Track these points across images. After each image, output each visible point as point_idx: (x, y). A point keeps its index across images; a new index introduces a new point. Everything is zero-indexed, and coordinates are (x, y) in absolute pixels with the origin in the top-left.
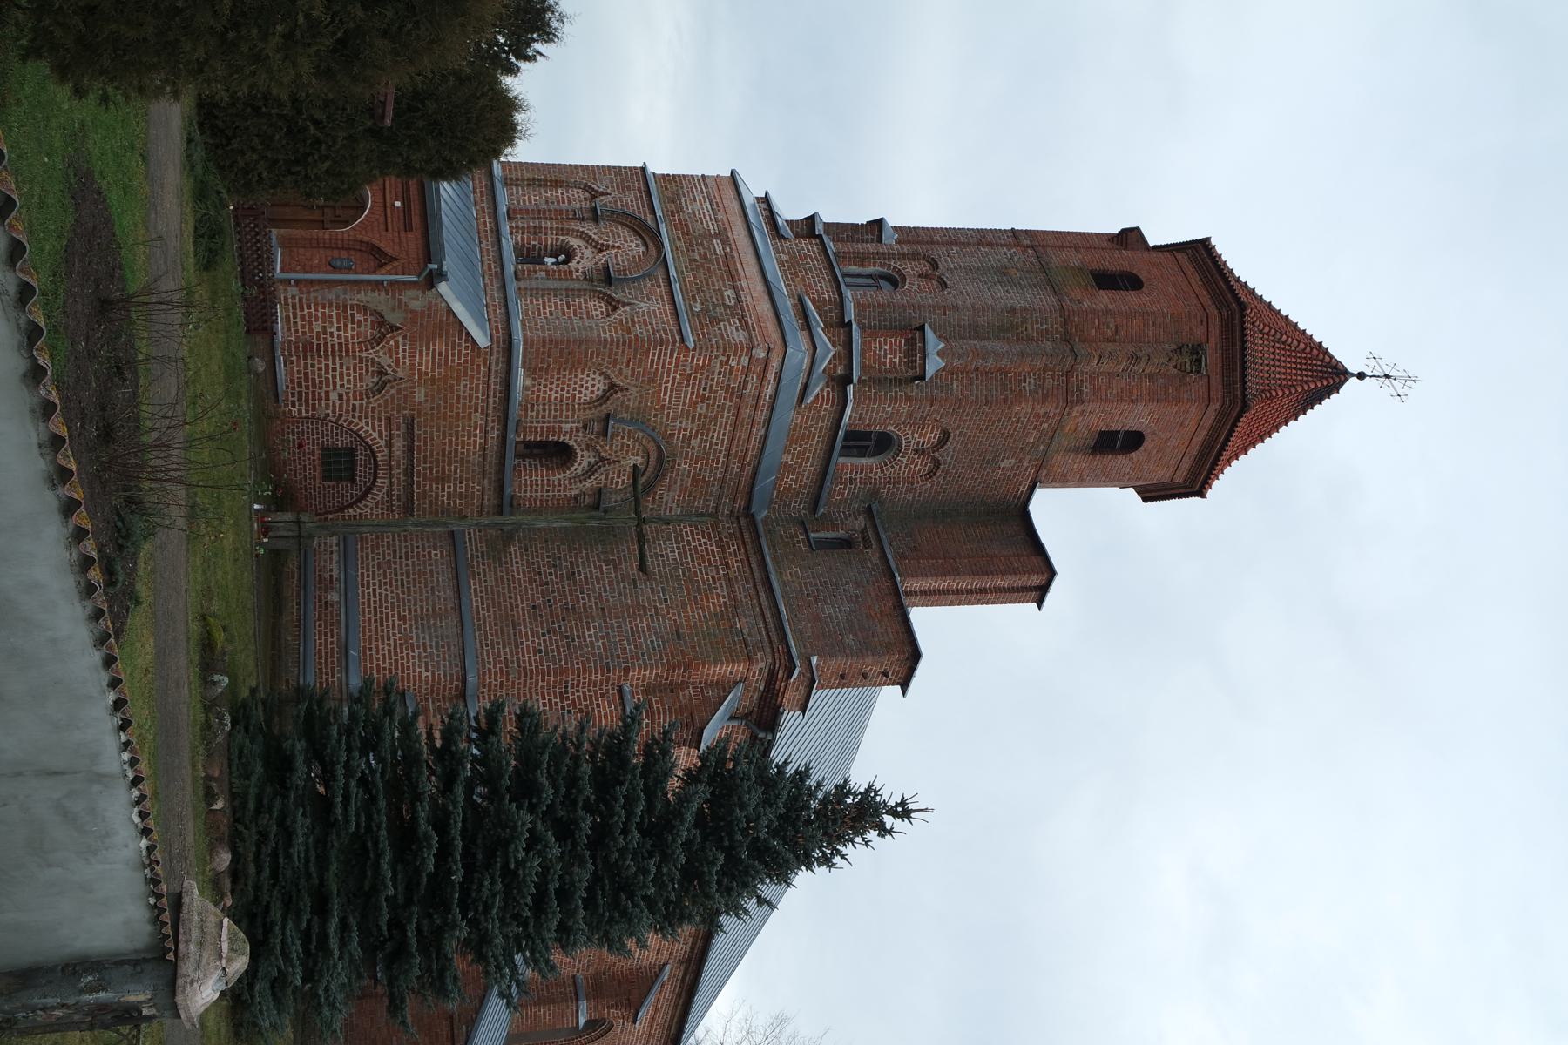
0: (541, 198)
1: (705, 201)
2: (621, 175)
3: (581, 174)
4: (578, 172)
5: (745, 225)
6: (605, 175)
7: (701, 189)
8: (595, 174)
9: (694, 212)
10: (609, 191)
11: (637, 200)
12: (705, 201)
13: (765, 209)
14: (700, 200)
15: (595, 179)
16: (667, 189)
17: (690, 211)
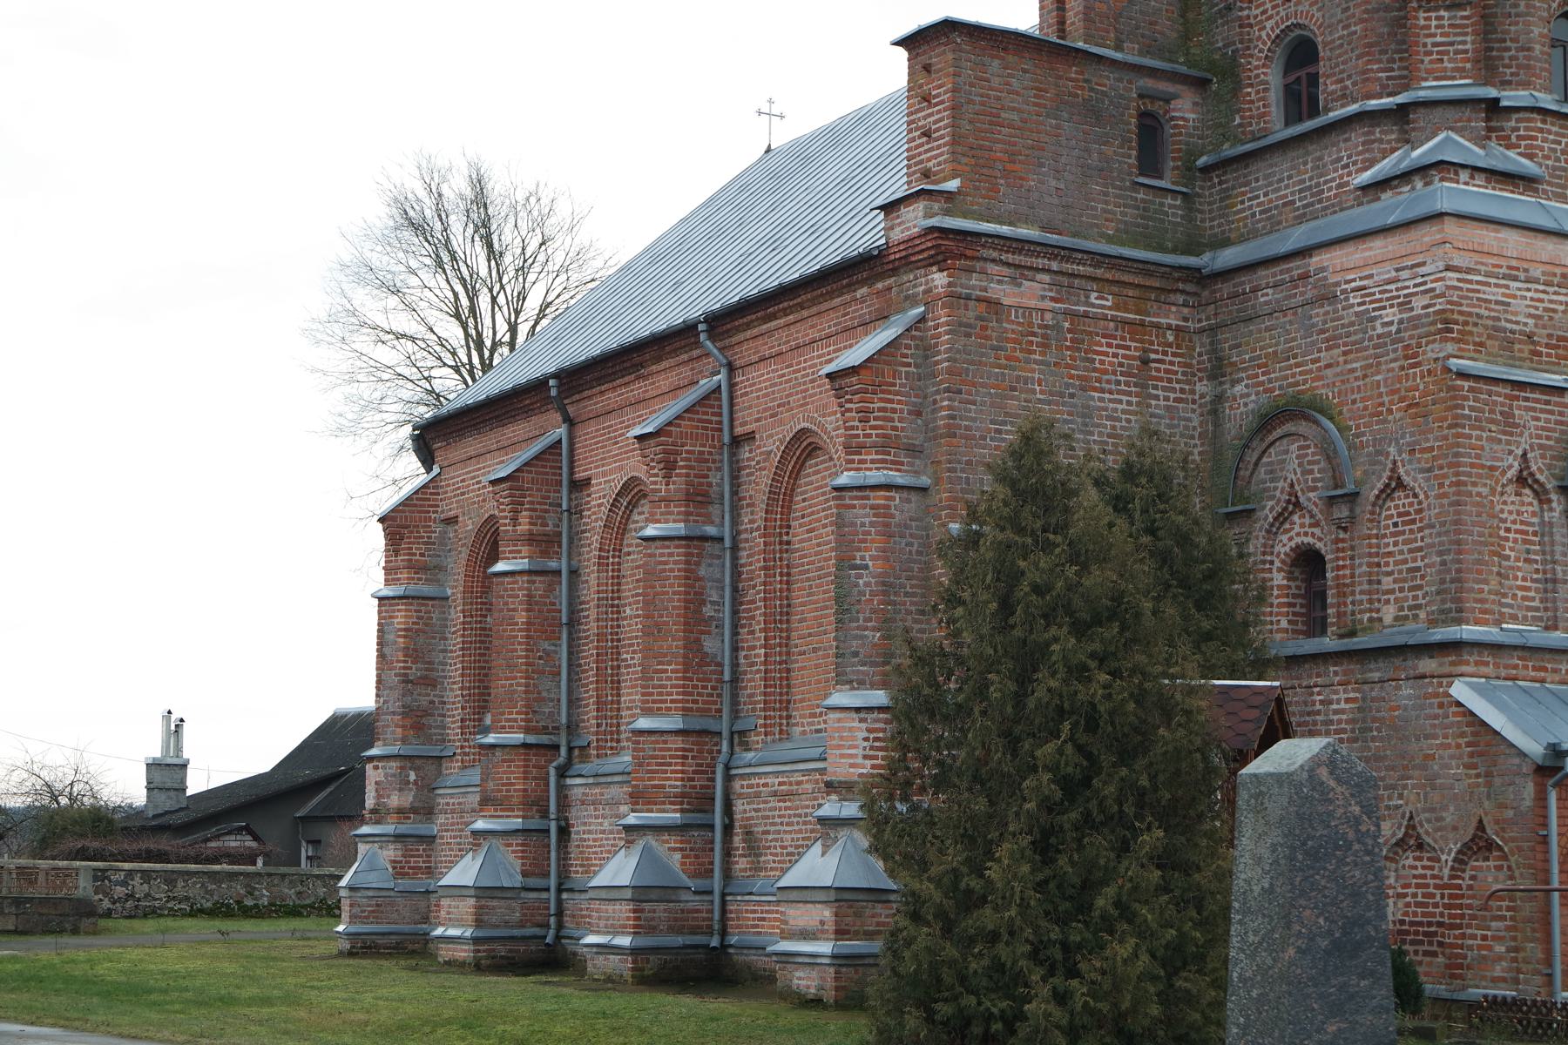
0: (1519, 569)
1: (1507, 287)
2: (1477, 419)
3: (1485, 491)
4: (1479, 494)
5: (1555, 239)
6: (1482, 448)
7: (1478, 282)
8: (1482, 466)
9: (1530, 316)
10: (1520, 452)
11: (1534, 409)
12: (1507, 287)
13: (1472, 177)
14: (1504, 295)
15: (1492, 468)
16: (1481, 344)
17: (1531, 321)
